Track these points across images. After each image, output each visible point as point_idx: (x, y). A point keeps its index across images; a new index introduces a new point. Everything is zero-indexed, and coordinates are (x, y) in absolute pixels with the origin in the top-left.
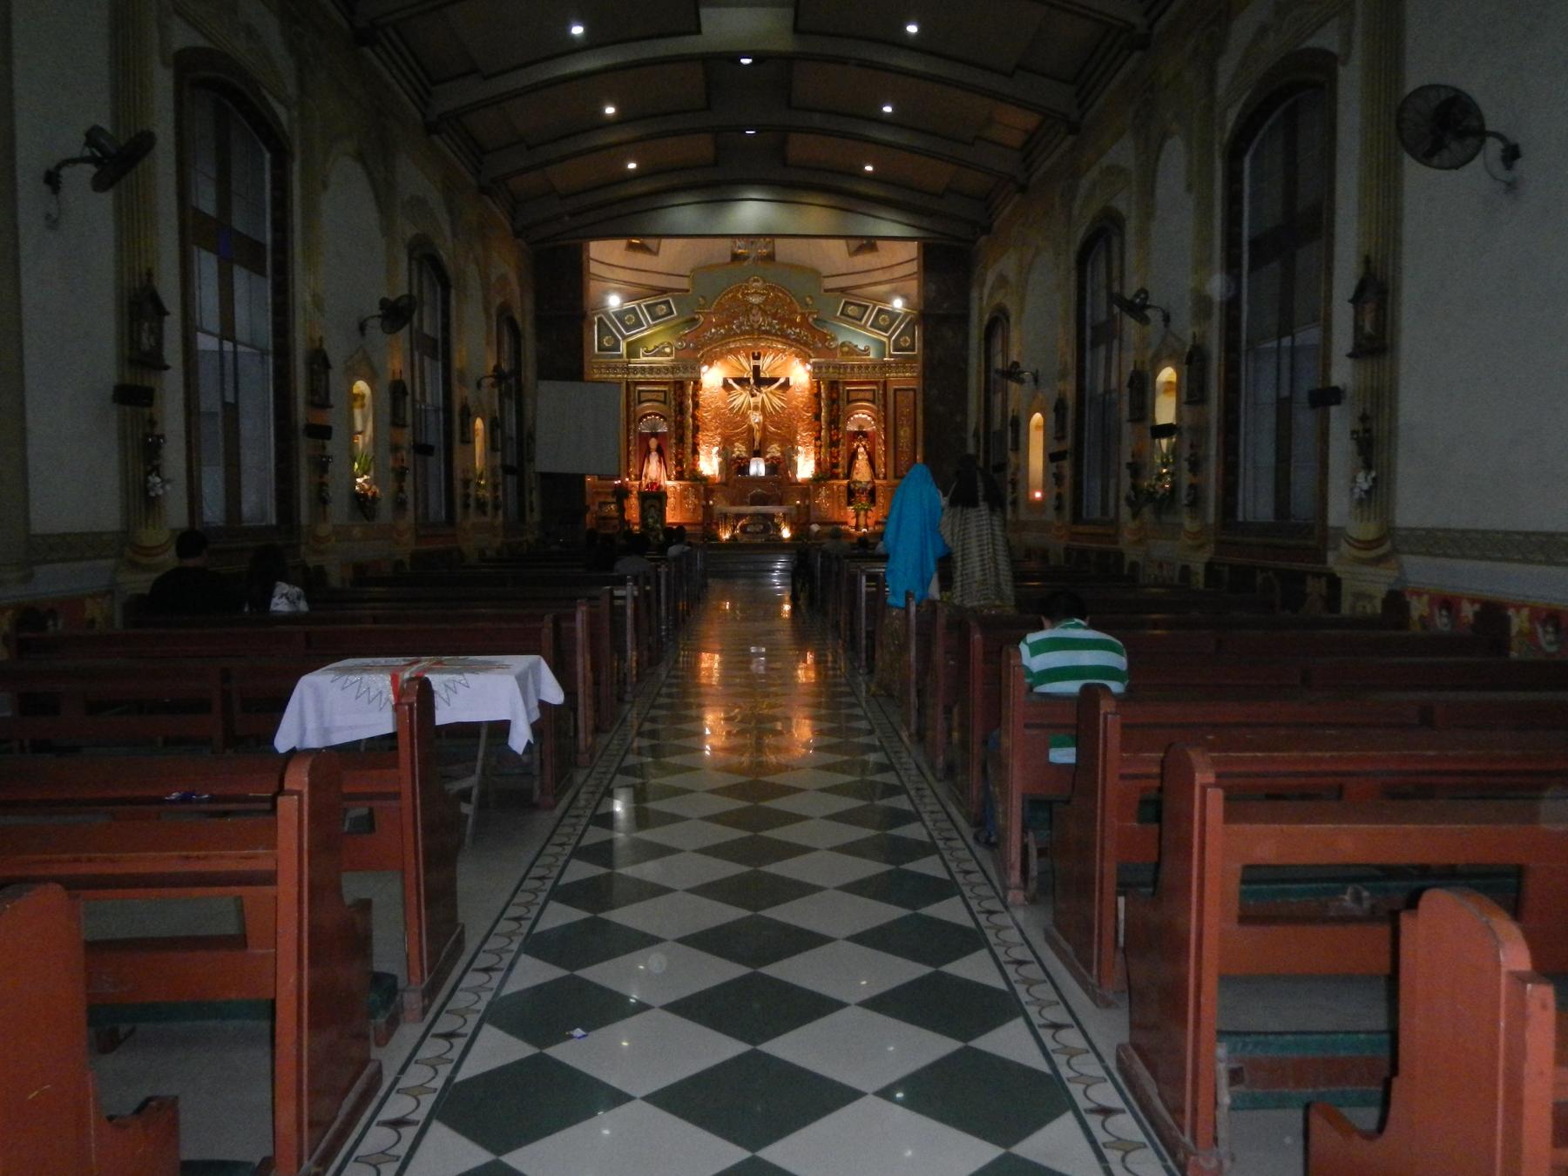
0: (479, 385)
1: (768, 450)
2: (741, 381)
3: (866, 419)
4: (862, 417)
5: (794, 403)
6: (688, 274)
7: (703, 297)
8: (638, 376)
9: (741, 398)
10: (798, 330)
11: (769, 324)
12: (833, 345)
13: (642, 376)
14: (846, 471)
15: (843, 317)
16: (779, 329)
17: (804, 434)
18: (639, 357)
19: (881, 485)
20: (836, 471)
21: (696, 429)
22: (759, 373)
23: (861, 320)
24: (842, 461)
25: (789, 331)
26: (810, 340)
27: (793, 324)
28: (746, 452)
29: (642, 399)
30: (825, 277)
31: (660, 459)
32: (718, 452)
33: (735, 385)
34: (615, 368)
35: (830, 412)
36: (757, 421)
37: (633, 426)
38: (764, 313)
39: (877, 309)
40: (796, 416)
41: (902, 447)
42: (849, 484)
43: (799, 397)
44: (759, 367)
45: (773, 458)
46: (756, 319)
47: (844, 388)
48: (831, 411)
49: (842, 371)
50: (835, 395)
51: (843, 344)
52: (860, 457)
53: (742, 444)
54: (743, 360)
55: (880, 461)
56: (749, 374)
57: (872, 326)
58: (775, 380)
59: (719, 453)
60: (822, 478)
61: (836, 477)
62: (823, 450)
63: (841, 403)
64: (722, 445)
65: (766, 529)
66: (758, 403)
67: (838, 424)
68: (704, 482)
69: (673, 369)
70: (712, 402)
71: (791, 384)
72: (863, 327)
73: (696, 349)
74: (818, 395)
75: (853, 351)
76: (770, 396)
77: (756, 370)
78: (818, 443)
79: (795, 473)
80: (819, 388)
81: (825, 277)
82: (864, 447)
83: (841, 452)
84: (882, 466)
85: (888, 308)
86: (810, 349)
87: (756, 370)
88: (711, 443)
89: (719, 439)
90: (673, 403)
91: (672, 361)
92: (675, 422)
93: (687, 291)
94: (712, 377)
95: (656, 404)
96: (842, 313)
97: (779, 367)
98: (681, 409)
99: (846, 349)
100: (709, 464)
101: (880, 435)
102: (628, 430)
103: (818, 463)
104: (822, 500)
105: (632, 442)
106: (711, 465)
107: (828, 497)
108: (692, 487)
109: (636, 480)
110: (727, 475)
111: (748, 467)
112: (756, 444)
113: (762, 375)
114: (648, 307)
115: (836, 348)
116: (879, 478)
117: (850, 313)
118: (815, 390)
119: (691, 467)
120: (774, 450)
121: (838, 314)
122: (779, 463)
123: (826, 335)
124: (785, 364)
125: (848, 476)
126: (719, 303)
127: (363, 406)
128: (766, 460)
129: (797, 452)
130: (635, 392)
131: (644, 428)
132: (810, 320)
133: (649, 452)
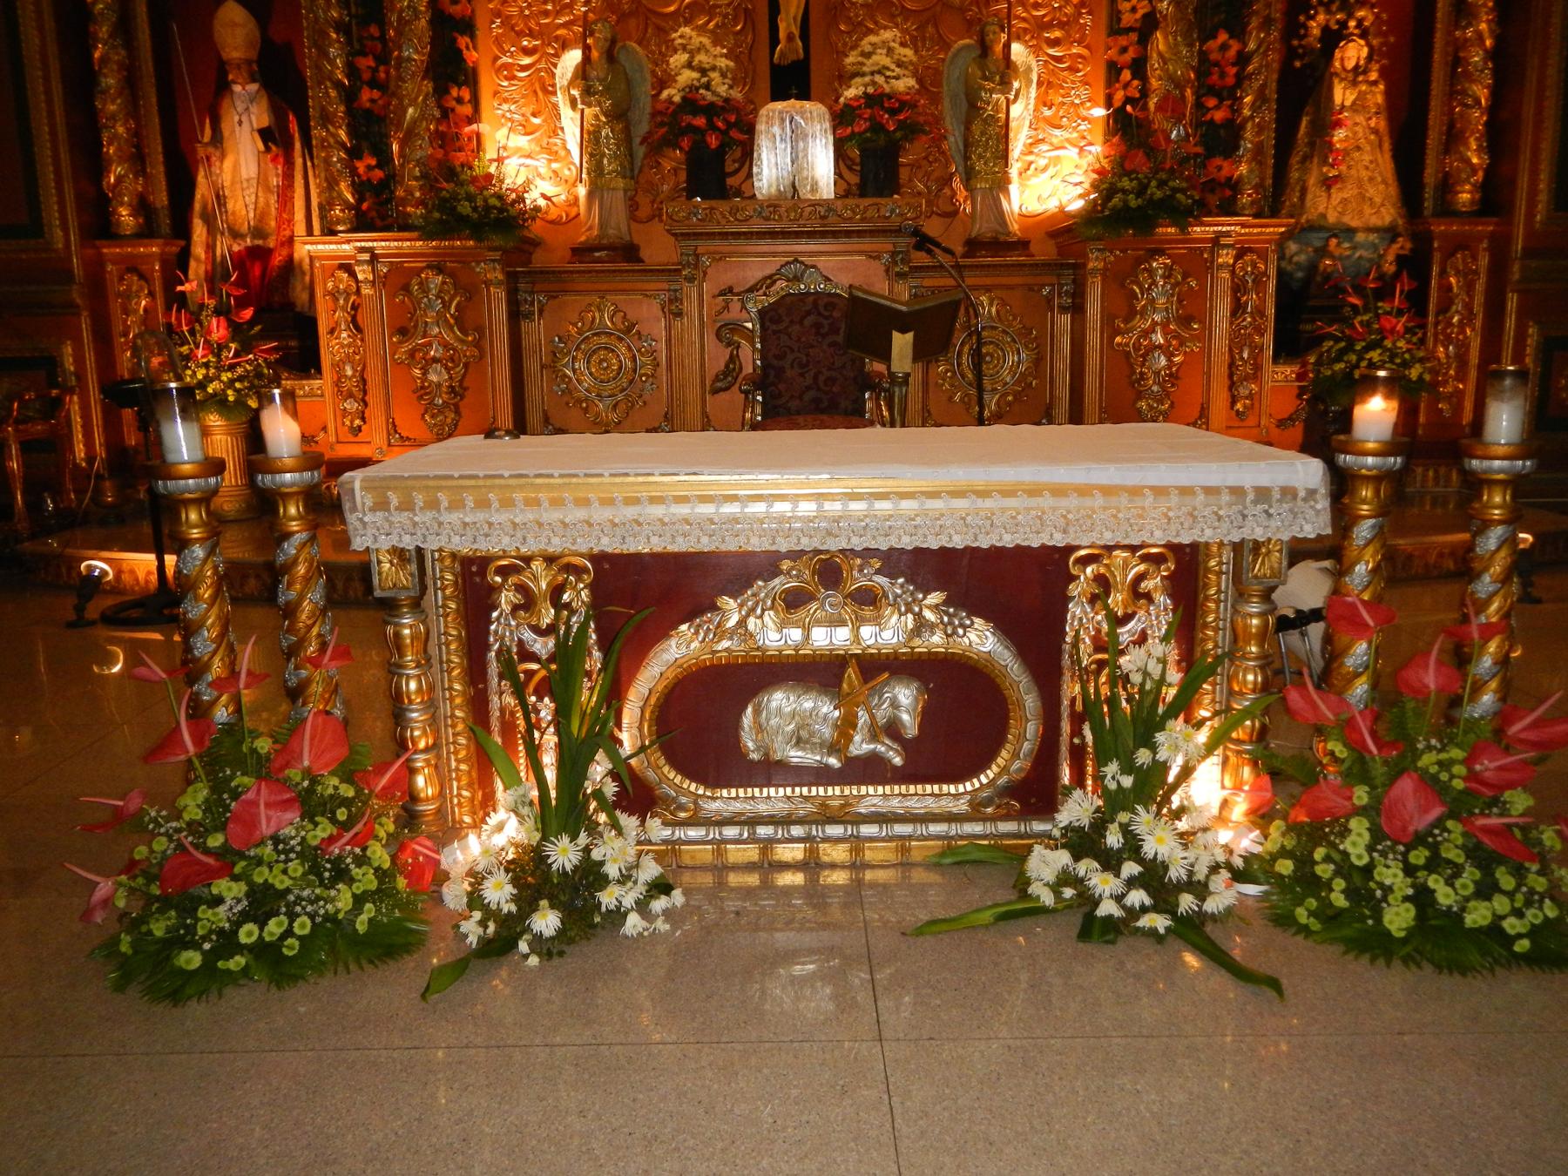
1: (852, 58)
20: (1223, 168)
31: (277, 112)
32: (583, 72)
45: (875, 100)
52: (1342, 95)
62: (1160, 41)
64: (602, 32)
68: (497, 241)
79: (1002, 183)
106: (552, 154)
109: (147, 232)
111: (748, 154)
112: (787, 24)
122: (911, 130)
128: (841, 118)
133: (223, 88)
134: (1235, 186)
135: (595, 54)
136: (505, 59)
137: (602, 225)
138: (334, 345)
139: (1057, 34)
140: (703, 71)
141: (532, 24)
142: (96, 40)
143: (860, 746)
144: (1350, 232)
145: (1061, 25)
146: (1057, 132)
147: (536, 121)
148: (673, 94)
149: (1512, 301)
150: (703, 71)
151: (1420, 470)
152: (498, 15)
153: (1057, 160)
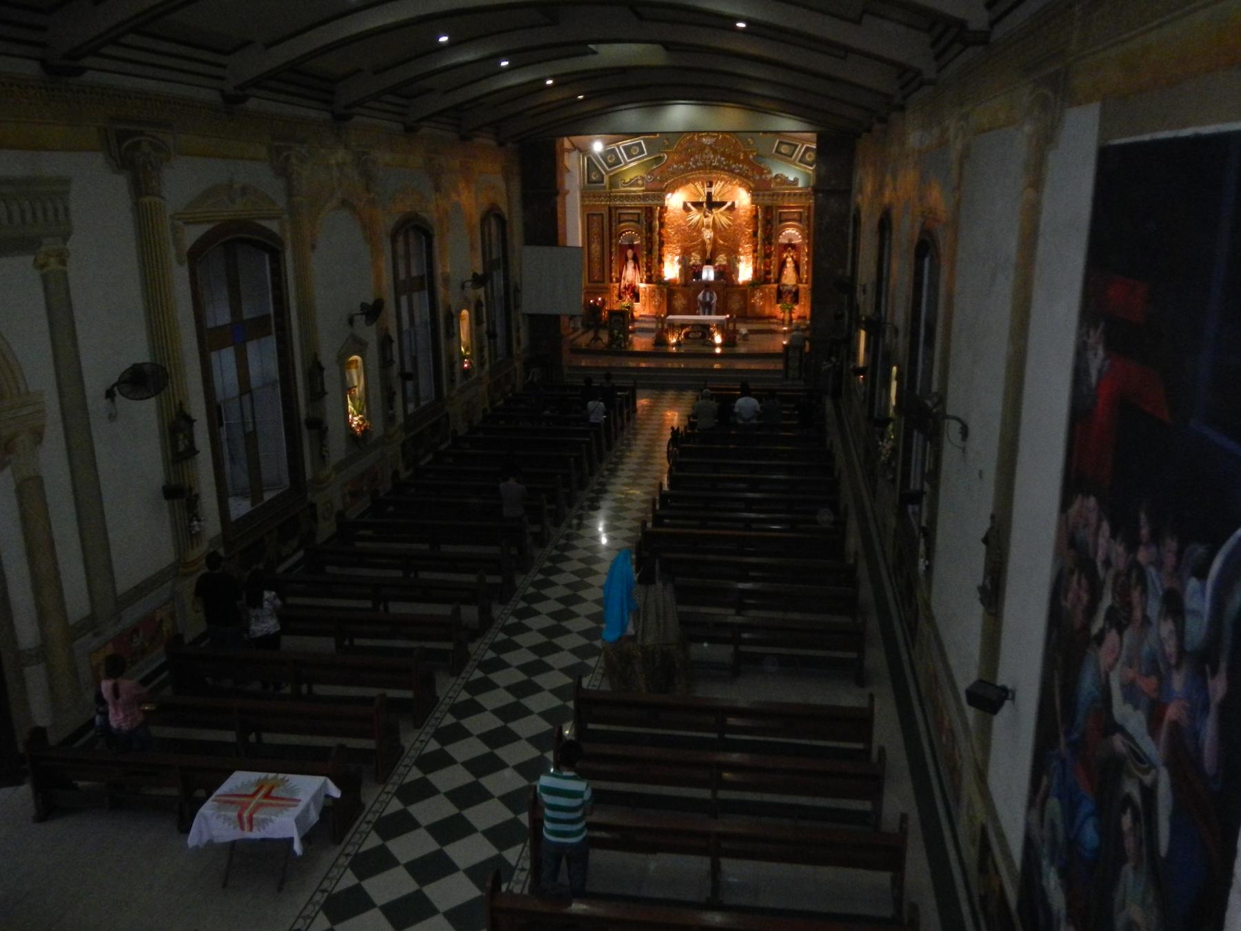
0: (463, 287)
1: (717, 259)
2: (696, 204)
3: (795, 234)
4: (792, 233)
5: (738, 221)
8: (617, 203)
9: (696, 216)
10: (741, 166)
11: (719, 161)
12: (769, 177)
13: (621, 203)
14: (777, 277)
15: (777, 154)
16: (726, 165)
17: (746, 246)
19: (805, 288)
20: (768, 277)
21: (662, 244)
23: (791, 156)
24: (774, 269)
25: (734, 166)
26: (750, 173)
27: (737, 160)
28: (700, 260)
29: (621, 220)
33: (692, 208)
34: (600, 197)
35: (764, 232)
36: (708, 237)
37: (614, 241)
38: (715, 152)
39: (805, 147)
40: (740, 231)
42: (778, 287)
43: (742, 216)
44: (711, 193)
45: (720, 266)
46: (707, 157)
48: (767, 229)
49: (775, 197)
50: (769, 217)
51: (777, 176)
52: (788, 265)
53: (698, 254)
54: (699, 187)
55: (804, 268)
56: (703, 199)
57: (800, 161)
58: (724, 203)
59: (680, 262)
60: (757, 284)
61: (767, 281)
62: (759, 261)
63: (774, 223)
65: (704, 336)
67: (771, 239)
69: (645, 197)
70: (675, 221)
71: (736, 206)
72: (793, 163)
73: (662, 181)
74: (756, 217)
75: (785, 181)
77: (709, 195)
78: (755, 255)
80: (757, 210)
82: (792, 257)
83: (773, 262)
84: (805, 273)
86: (750, 181)
87: (709, 195)
88: (673, 253)
89: (679, 251)
90: (645, 223)
91: (644, 191)
92: (646, 238)
94: (675, 201)
95: (632, 223)
96: (778, 151)
98: (650, 229)
100: (671, 270)
101: (804, 249)
103: (755, 271)
104: (757, 300)
105: (614, 253)
107: (761, 298)
108: (658, 288)
110: (686, 277)
113: (714, 199)
114: (624, 148)
115: (770, 180)
116: (801, 283)
117: (783, 151)
118: (754, 213)
119: (657, 273)
120: (722, 259)
121: (774, 150)
123: (763, 169)
125: (778, 280)
127: (357, 367)
128: (715, 268)
129: (739, 261)
130: (615, 215)
131: (622, 241)
132: (751, 157)
133: (627, 260)
134: (770, 279)
138: (642, 298)
140: (696, 260)
144: (787, 285)
148: (691, 263)
150: (696, 260)
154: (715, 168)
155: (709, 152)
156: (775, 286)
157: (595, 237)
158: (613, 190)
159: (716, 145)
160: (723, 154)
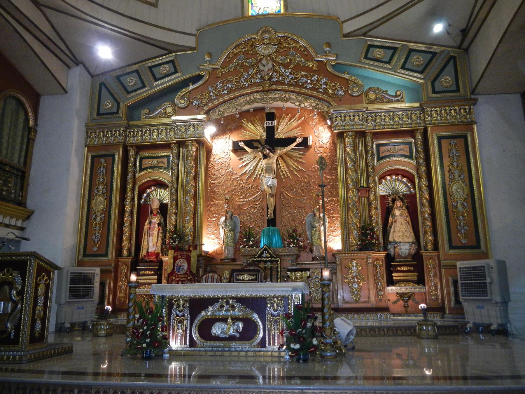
6: (195, 33)
7: (210, 55)
16: (292, 79)
18: (140, 120)
22: (274, 135)
30: (343, 22)
32: (225, 221)
33: (246, 148)
36: (269, 183)
37: (129, 194)
41: (456, 207)
47: (373, 142)
51: (370, 89)
58: (291, 140)
66: (272, 163)
71: (310, 143)
76: (286, 158)
77: (270, 131)
81: (343, 22)
85: (422, 47)
87: (270, 131)
93: (192, 49)
97: (296, 128)
99: (372, 96)
102: (123, 199)
106: (217, 238)
113: (277, 136)
124: (303, 125)
126: (228, 57)
135: (228, 218)
136: (210, 219)
137: (228, 254)
139: (332, 212)
141: (216, 212)
142: (125, 216)
143: (231, 332)
145: (333, 210)
146: (334, 233)
147: (216, 232)
149: (443, 271)
151: (429, 315)
152: (209, 210)
153: (334, 239)
154: (277, 83)
155: (268, 64)
156: (382, 255)
157: (101, 188)
158: (131, 123)
159: (276, 56)
160: (286, 66)
